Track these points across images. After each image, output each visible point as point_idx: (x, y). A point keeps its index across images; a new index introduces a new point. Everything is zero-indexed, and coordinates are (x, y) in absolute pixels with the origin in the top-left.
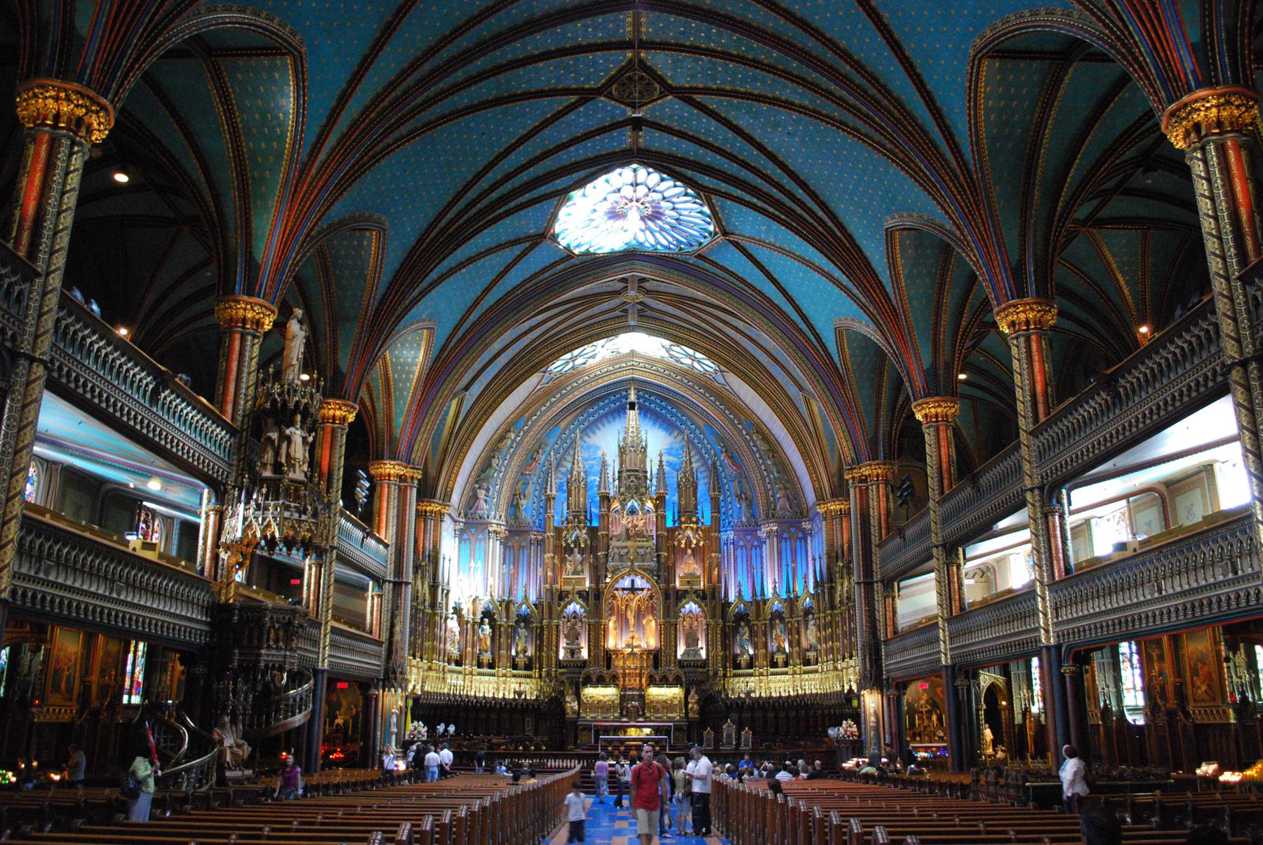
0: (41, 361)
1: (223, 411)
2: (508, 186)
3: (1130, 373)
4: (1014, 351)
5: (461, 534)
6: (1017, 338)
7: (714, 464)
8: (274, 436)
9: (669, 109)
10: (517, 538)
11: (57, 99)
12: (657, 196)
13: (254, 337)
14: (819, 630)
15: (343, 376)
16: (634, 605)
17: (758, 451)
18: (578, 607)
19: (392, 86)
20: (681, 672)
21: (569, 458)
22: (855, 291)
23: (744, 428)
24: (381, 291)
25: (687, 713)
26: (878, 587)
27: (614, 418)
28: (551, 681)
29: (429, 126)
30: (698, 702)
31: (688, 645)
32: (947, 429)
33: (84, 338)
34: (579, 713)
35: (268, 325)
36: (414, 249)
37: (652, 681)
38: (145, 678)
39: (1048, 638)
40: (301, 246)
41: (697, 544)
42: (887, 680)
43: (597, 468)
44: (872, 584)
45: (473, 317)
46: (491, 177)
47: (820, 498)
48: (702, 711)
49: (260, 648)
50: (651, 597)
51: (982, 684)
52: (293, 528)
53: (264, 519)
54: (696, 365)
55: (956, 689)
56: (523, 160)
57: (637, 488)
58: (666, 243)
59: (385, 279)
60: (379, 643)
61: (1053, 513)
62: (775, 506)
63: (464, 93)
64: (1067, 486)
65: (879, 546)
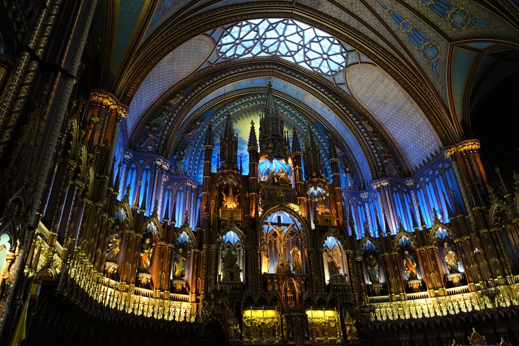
10: (176, 184)
17: (366, 131)
25: (345, 336)
27: (250, 114)
28: (210, 304)
31: (331, 272)
34: (241, 337)
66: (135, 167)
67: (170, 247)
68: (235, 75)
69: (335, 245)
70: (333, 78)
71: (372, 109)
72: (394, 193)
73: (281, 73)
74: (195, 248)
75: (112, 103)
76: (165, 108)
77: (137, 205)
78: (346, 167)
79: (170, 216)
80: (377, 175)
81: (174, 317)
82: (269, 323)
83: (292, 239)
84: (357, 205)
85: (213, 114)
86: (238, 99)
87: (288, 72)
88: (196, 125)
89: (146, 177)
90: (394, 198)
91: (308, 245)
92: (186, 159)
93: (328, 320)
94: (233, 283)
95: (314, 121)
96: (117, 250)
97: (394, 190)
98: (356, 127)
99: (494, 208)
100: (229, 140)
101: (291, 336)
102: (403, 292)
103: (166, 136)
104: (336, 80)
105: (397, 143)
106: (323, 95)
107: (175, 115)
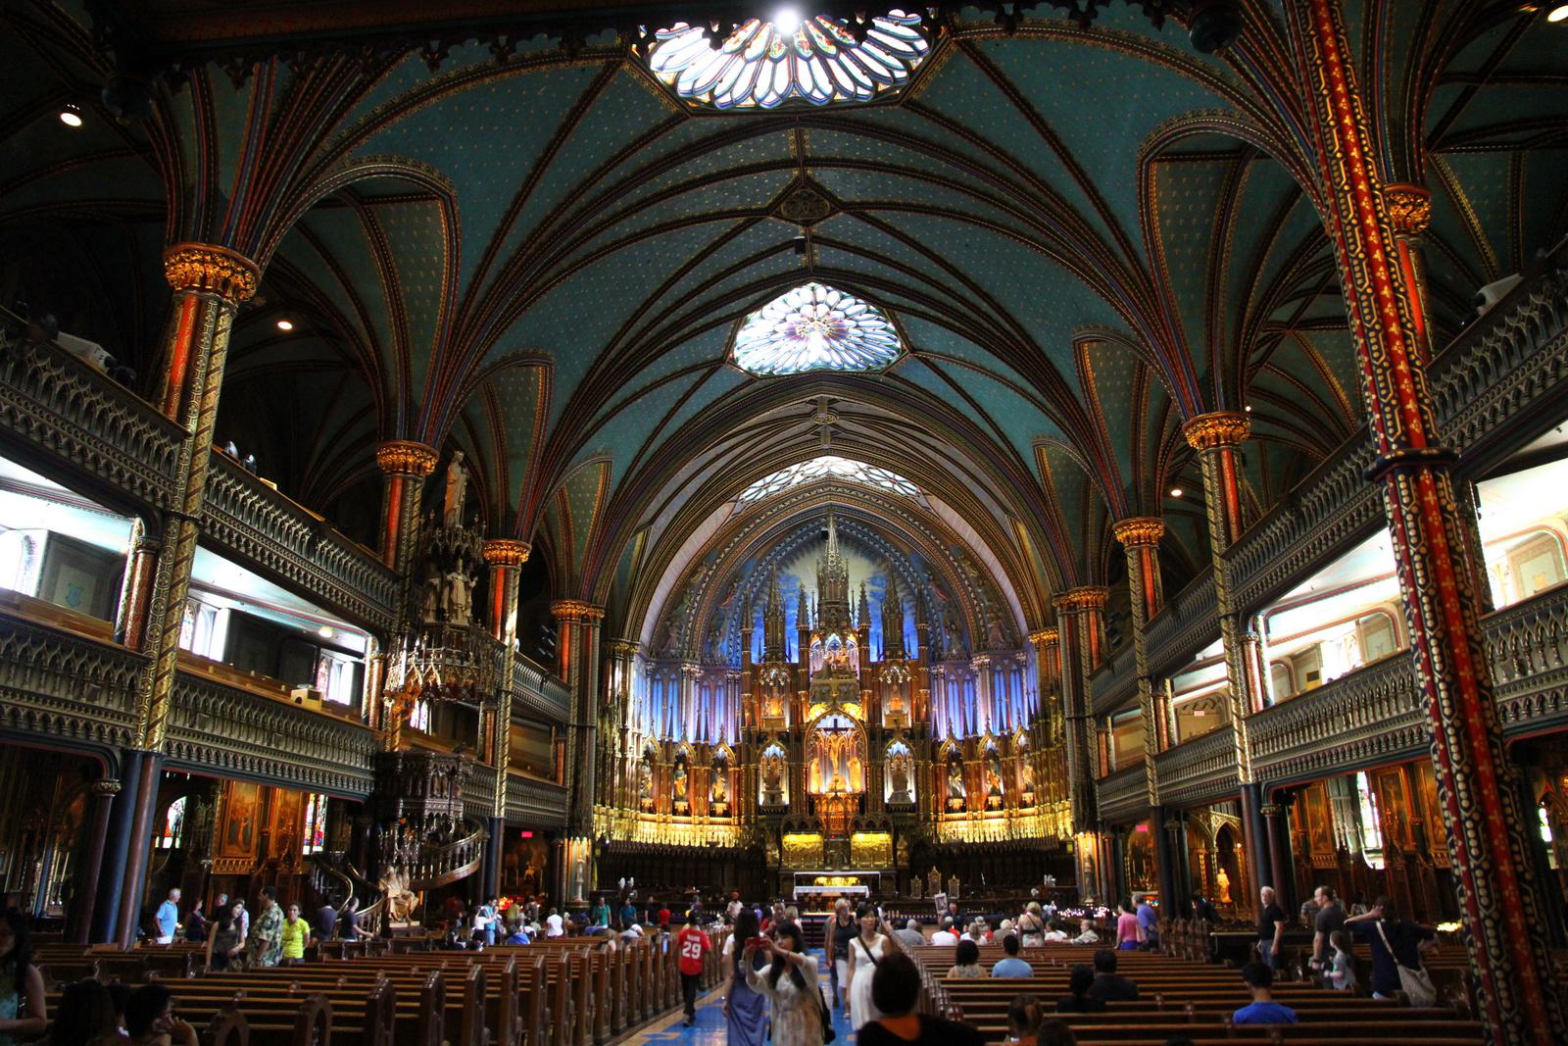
0: (195, 521)
1: (386, 559)
2: (681, 312)
3: (1311, 491)
4: (1205, 468)
5: (652, 676)
6: (1207, 454)
7: (920, 592)
8: (436, 581)
9: (842, 225)
11: (202, 262)
12: (839, 315)
13: (416, 481)
14: (1035, 769)
15: (515, 515)
16: (836, 746)
18: (778, 749)
19: (548, 221)
20: (889, 817)
21: (767, 590)
22: (1049, 406)
24: (551, 428)
25: (895, 861)
26: (1091, 723)
29: (590, 258)
30: (907, 849)
31: (895, 787)
32: (1150, 551)
33: (236, 494)
34: (780, 862)
35: (430, 465)
36: (584, 382)
37: (858, 827)
38: (326, 829)
39: (1246, 777)
40: (462, 388)
41: (904, 679)
42: (1102, 822)
43: (796, 601)
44: (1083, 719)
45: (653, 448)
46: (661, 304)
47: (1033, 628)
48: (912, 859)
49: (424, 796)
50: (856, 737)
51: (1214, 825)
52: (455, 675)
53: (426, 667)
54: (897, 487)
55: (1166, 832)
56: (694, 285)
57: (838, 622)
58: (853, 362)
59: (555, 414)
60: (563, 791)
61: (1248, 641)
63: (625, 222)
64: (1264, 612)
65: (1090, 678)
78: (952, 623)
79: (703, 736)
80: (978, 646)
89: (672, 689)
95: (906, 550)
96: (650, 785)
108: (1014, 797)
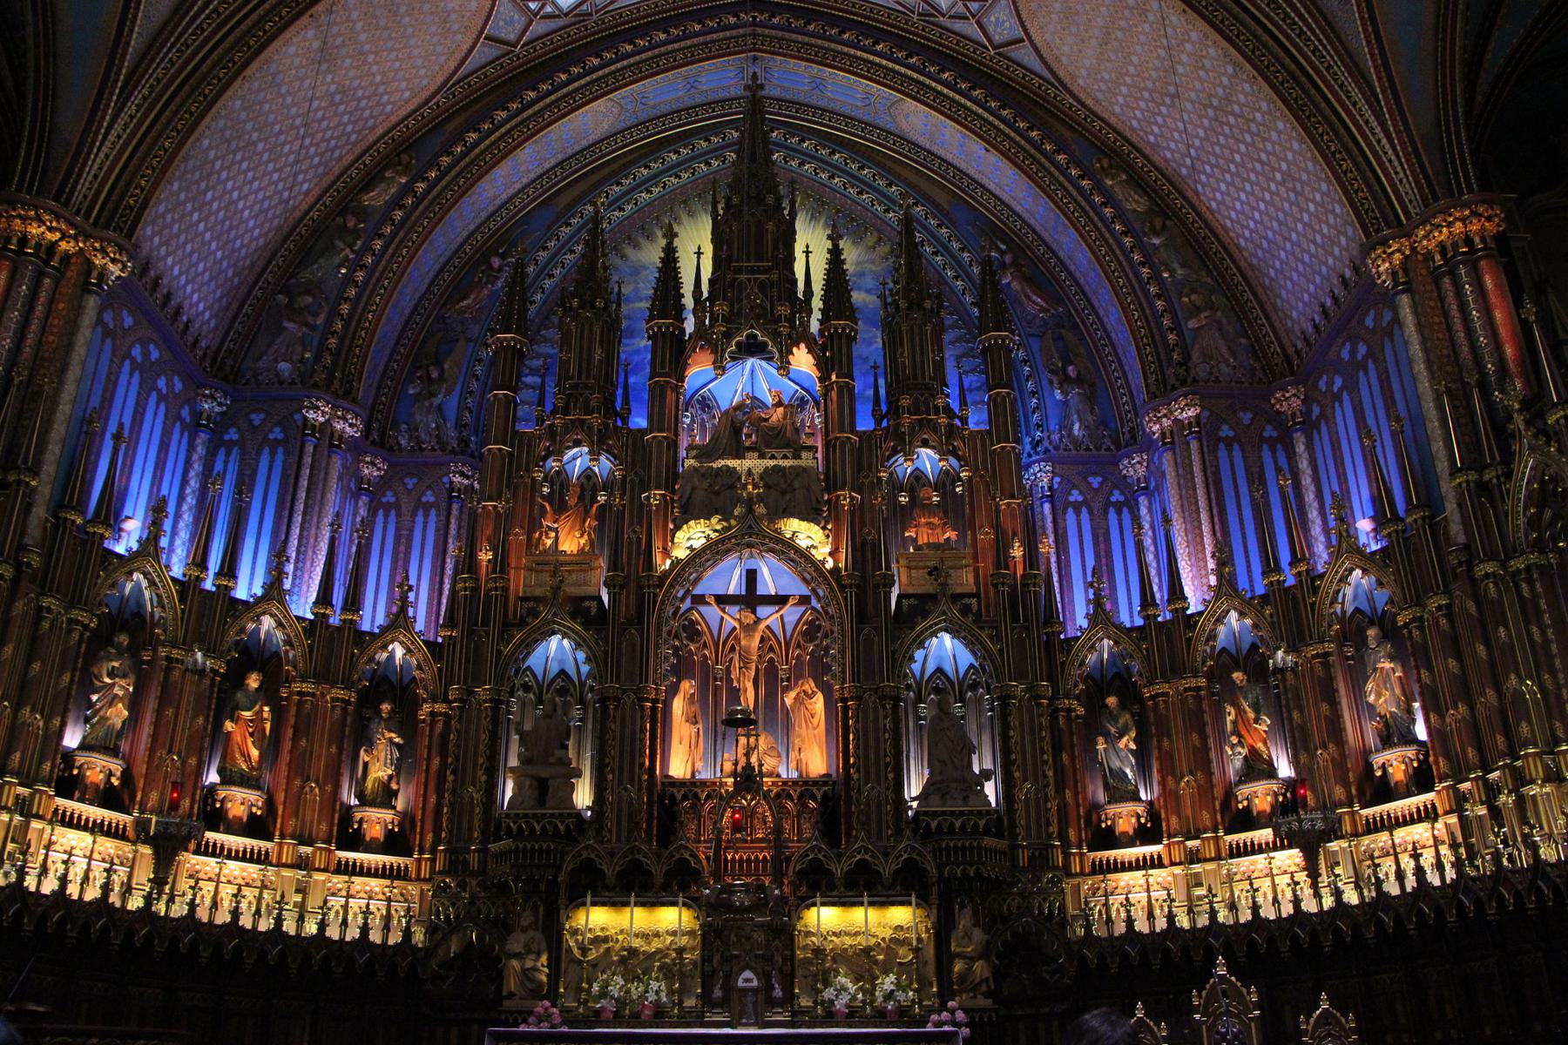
17: (1120, 215)
18: (566, 642)
23: (1074, 161)
30: (984, 954)
50: (811, 632)
62: (1186, 357)
66: (235, 437)
67: (337, 700)
68: (607, 70)
69: (971, 666)
70: (979, 23)
71: (1135, 123)
72: (1222, 446)
73: (787, 35)
74: (434, 699)
75: (58, 235)
76: (344, 228)
77: (197, 565)
81: (322, 925)
82: (659, 951)
83: (811, 654)
84: (1107, 505)
85: (554, 223)
86: (646, 155)
87: (811, 27)
88: (491, 266)
89: (269, 469)
90: (1217, 467)
91: (843, 672)
92: (448, 393)
93: (892, 939)
94: (544, 815)
95: (942, 199)
97: (1222, 434)
98: (1084, 203)
99: (1524, 473)
100: (581, 306)
101: (717, 993)
102: (1215, 830)
103: (348, 321)
104: (991, 29)
105: (1238, 246)
106: (951, 94)
107: (378, 244)
108: (1340, 765)
